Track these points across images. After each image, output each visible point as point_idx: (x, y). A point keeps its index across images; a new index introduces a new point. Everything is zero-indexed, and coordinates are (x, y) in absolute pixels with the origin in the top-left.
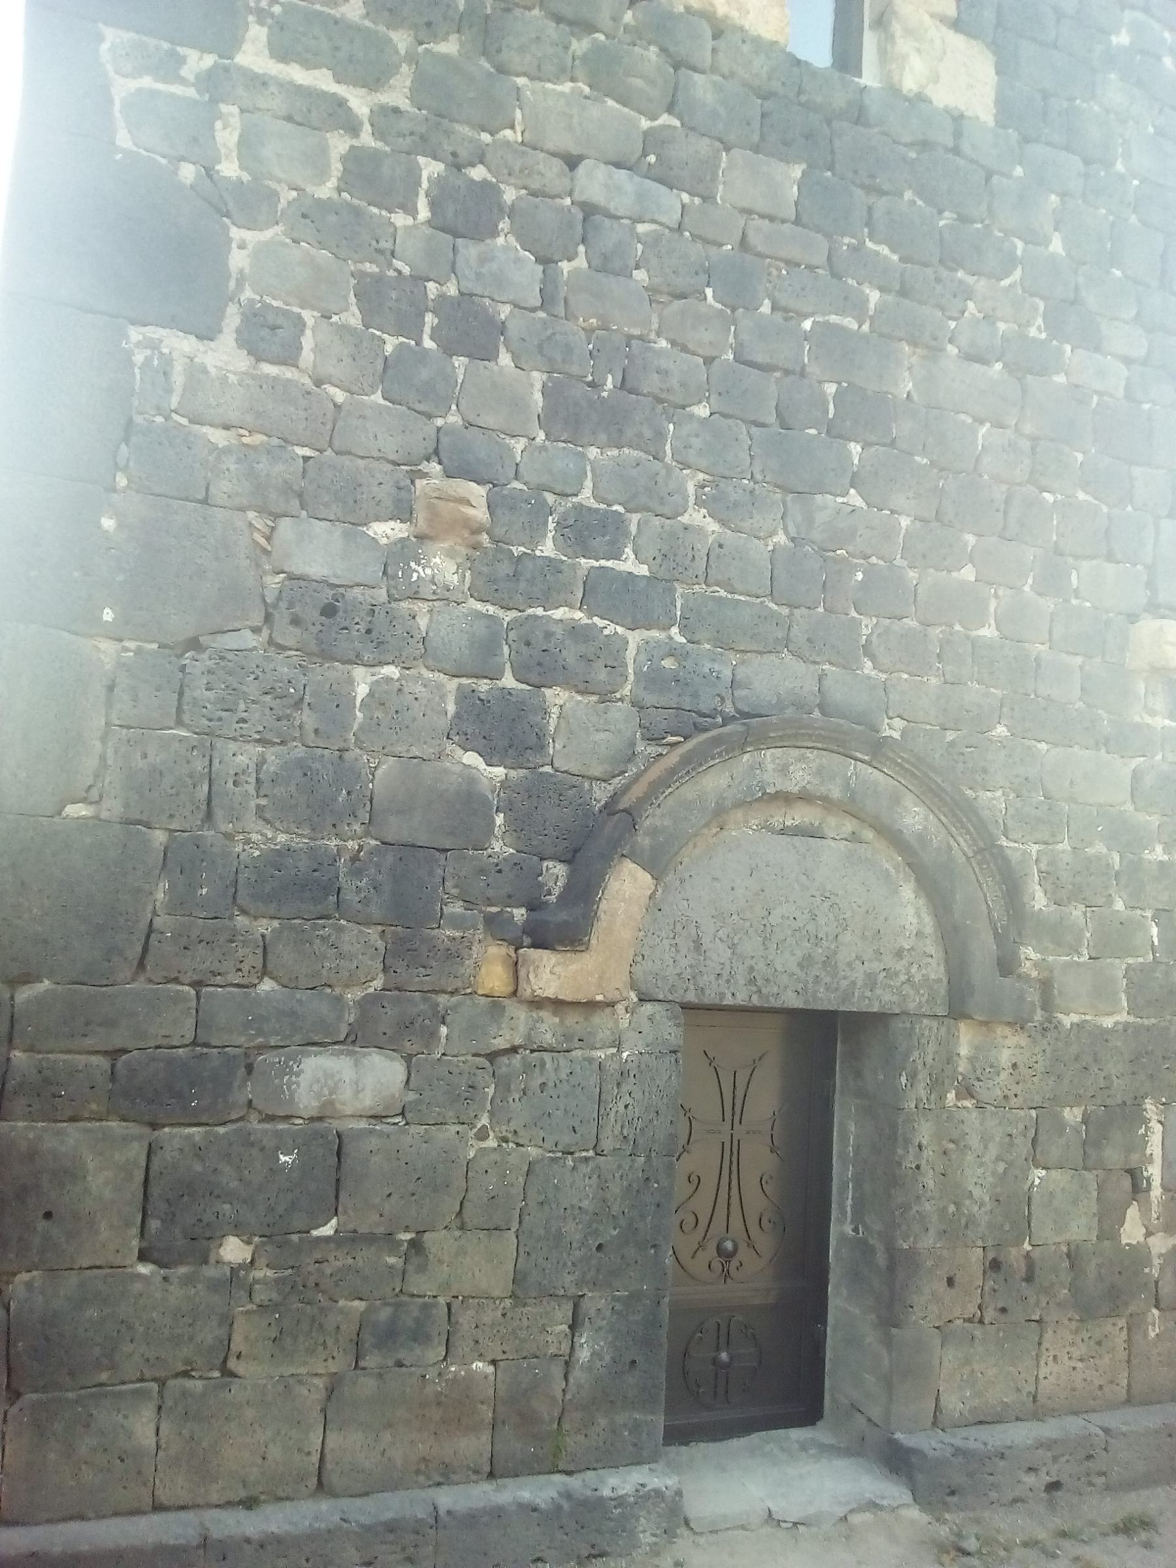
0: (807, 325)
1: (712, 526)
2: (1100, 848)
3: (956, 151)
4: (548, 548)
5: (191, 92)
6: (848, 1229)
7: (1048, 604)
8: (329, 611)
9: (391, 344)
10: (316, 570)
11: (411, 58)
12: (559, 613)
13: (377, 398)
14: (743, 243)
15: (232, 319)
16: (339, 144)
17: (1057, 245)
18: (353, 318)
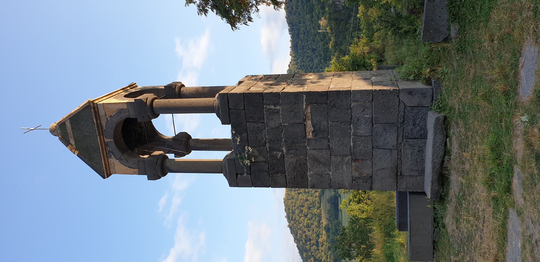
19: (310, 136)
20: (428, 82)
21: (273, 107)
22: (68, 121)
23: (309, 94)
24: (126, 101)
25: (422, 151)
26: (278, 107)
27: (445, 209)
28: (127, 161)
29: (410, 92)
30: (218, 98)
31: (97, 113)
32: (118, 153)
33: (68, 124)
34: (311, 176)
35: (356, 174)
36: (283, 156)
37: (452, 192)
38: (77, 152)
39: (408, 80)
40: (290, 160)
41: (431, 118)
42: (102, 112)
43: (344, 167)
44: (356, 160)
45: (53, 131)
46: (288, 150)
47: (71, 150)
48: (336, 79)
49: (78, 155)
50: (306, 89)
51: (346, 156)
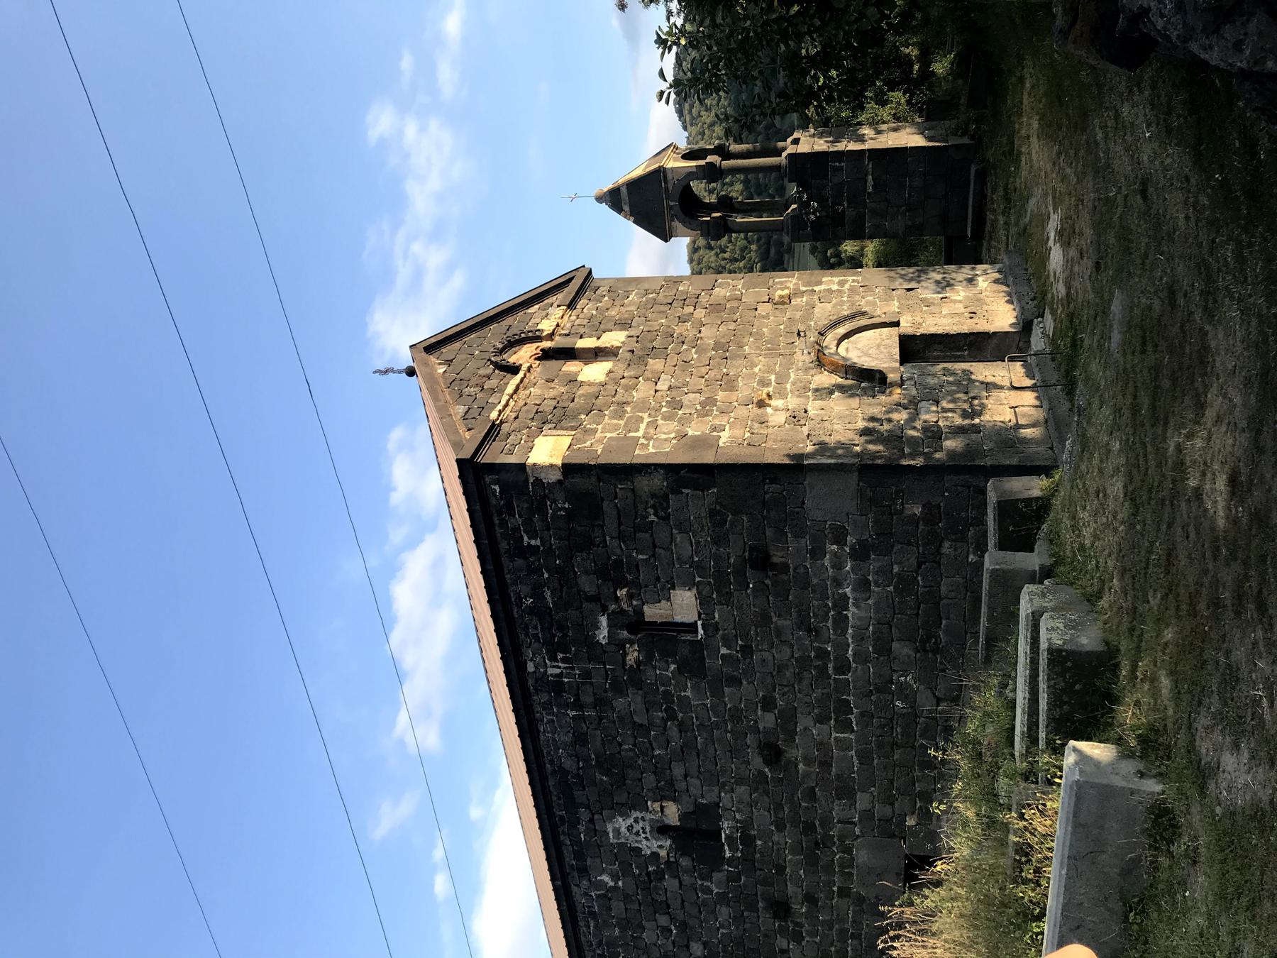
0: (695, 356)
1: (759, 367)
2: (845, 307)
3: (638, 337)
4: (771, 389)
5: (651, 442)
6: (966, 353)
7: (772, 318)
8: (794, 417)
9: (715, 412)
10: (783, 420)
11: (634, 413)
12: (788, 386)
13: (732, 414)
14: (675, 366)
15: (715, 434)
16: (660, 422)
17: (663, 321)
18: (710, 418)
19: (870, 189)
20: (972, 137)
21: (837, 164)
22: (625, 187)
23: (871, 151)
24: (695, 164)
25: (967, 199)
26: (843, 164)
27: (981, 245)
28: (690, 224)
29: (957, 147)
30: (786, 158)
31: (665, 177)
32: (683, 216)
33: (624, 190)
34: (869, 227)
35: (910, 223)
36: (843, 211)
37: (987, 230)
38: (632, 218)
39: (956, 135)
40: (850, 214)
41: (973, 169)
42: (670, 176)
43: (900, 217)
44: (909, 210)
45: (600, 199)
46: (849, 204)
47: (625, 217)
48: (893, 135)
49: (634, 222)
50: (866, 146)
51: (901, 207)
